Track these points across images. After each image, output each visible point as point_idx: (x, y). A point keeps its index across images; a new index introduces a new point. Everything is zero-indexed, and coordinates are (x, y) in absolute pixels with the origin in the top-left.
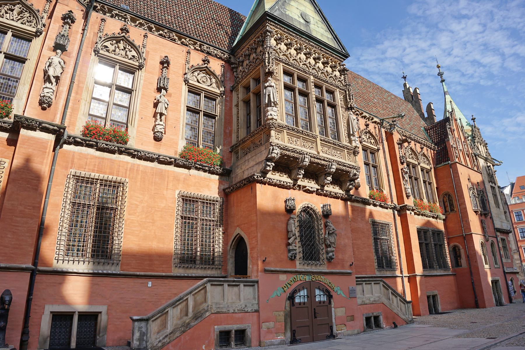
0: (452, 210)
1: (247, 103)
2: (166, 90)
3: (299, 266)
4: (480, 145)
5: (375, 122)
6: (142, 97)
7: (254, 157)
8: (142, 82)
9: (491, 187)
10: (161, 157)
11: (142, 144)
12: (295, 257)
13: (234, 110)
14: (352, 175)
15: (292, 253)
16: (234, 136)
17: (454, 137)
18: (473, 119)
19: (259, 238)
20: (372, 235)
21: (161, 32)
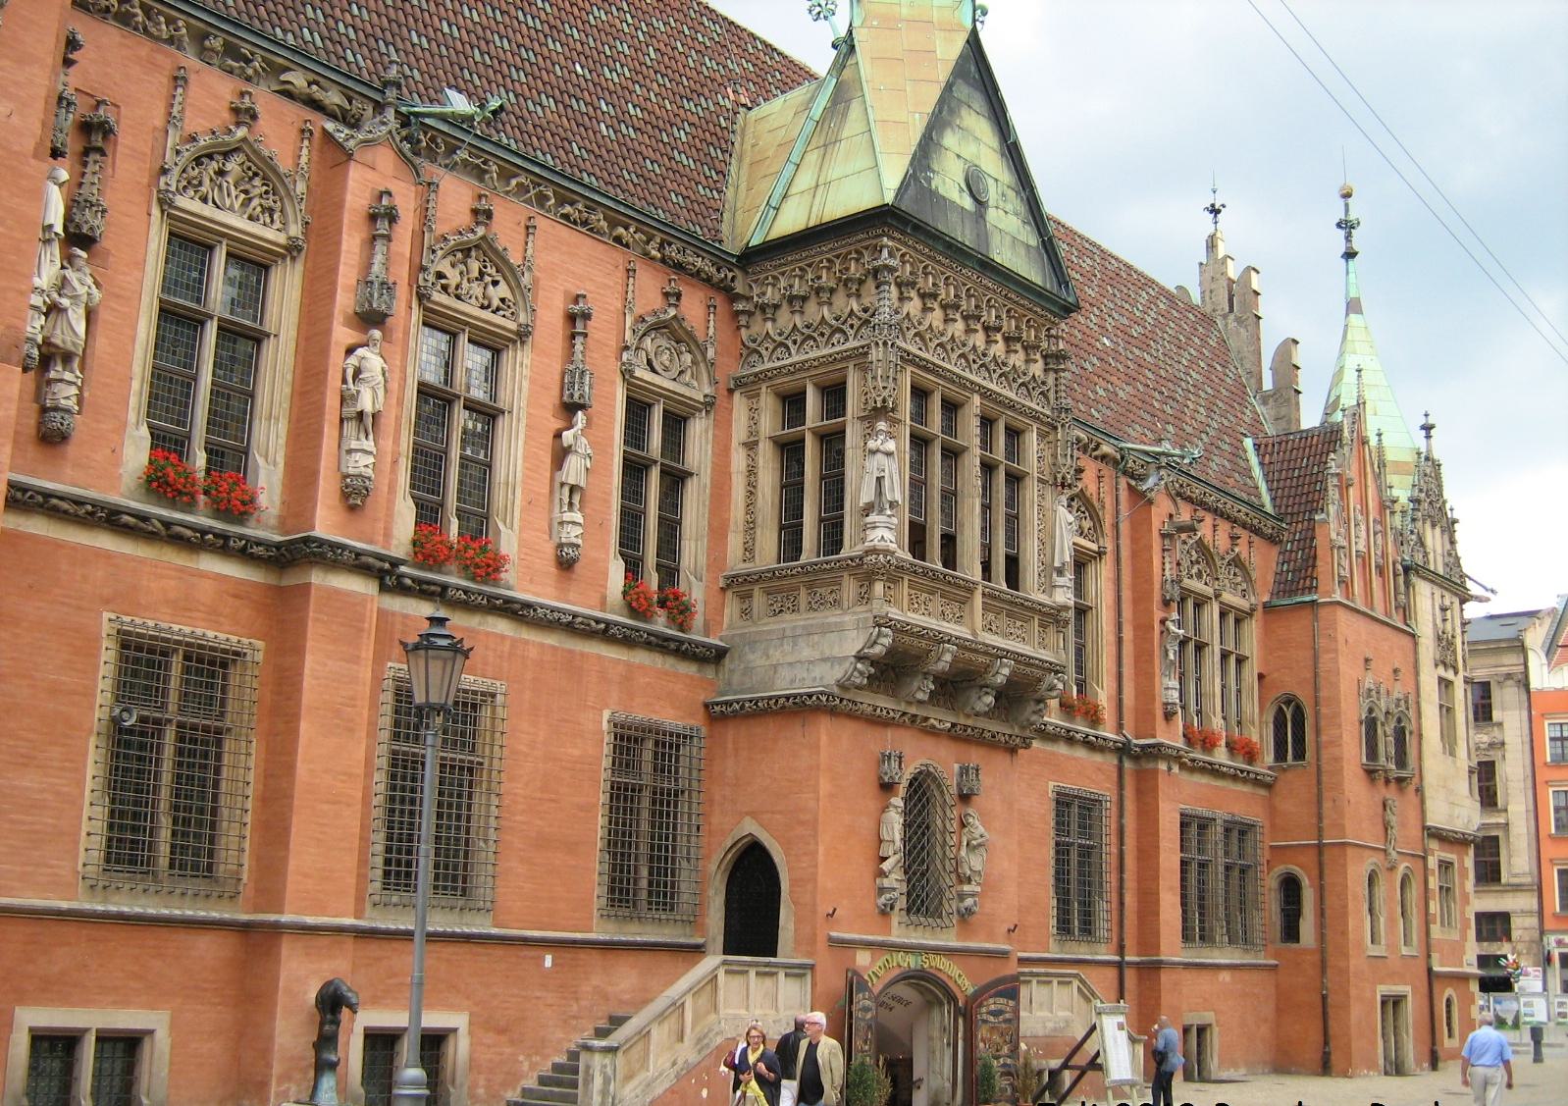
0: (1300, 754)
1: (790, 451)
3: (898, 934)
4: (1433, 526)
5: (1104, 457)
6: (527, 436)
7: (816, 637)
8: (525, 384)
9: (1441, 680)
10: (580, 619)
12: (892, 908)
13: (739, 460)
14: (1044, 686)
16: (735, 542)
17: (1344, 508)
18: (1428, 428)
19: (821, 858)
20: (1052, 833)
21: (568, 209)
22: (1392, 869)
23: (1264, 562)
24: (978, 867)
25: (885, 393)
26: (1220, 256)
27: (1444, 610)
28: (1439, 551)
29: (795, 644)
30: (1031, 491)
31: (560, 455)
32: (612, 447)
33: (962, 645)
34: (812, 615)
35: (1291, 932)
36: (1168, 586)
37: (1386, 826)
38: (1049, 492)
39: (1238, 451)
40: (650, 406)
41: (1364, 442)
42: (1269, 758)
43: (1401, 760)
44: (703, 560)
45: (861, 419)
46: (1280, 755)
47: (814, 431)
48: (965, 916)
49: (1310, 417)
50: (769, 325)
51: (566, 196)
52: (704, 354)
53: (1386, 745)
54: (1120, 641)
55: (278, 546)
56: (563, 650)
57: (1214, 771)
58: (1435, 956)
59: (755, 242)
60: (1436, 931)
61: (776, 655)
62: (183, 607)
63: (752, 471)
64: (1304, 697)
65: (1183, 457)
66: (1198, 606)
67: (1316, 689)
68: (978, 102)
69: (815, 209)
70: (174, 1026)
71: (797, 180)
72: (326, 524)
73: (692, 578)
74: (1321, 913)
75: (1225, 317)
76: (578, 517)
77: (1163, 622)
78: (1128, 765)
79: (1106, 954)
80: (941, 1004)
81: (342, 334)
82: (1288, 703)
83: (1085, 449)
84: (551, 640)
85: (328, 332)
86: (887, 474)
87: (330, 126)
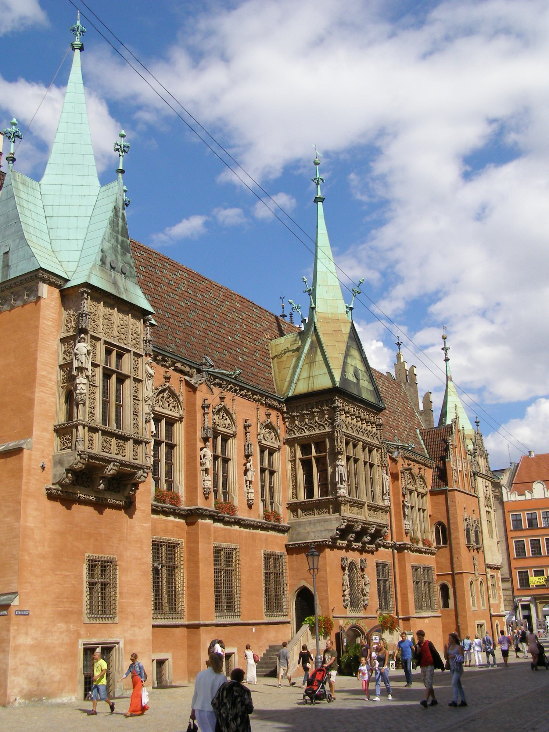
3: (349, 614)
4: (481, 457)
9: (487, 511)
14: (383, 532)
22: (477, 580)
23: (429, 474)
26: (402, 361)
28: (483, 466)
29: (315, 525)
30: (376, 469)
31: (246, 472)
35: (446, 604)
42: (435, 544)
43: (477, 542)
46: (438, 542)
48: (365, 607)
51: (239, 387)
53: (473, 538)
55: (188, 510)
57: (419, 551)
59: (290, 395)
60: (491, 599)
62: (165, 531)
64: (445, 521)
68: (355, 346)
69: (310, 385)
70: (173, 657)
71: (302, 374)
72: (201, 503)
75: (405, 384)
76: (252, 491)
77: (403, 502)
80: (360, 635)
81: (200, 444)
85: (195, 444)
87: (187, 378)
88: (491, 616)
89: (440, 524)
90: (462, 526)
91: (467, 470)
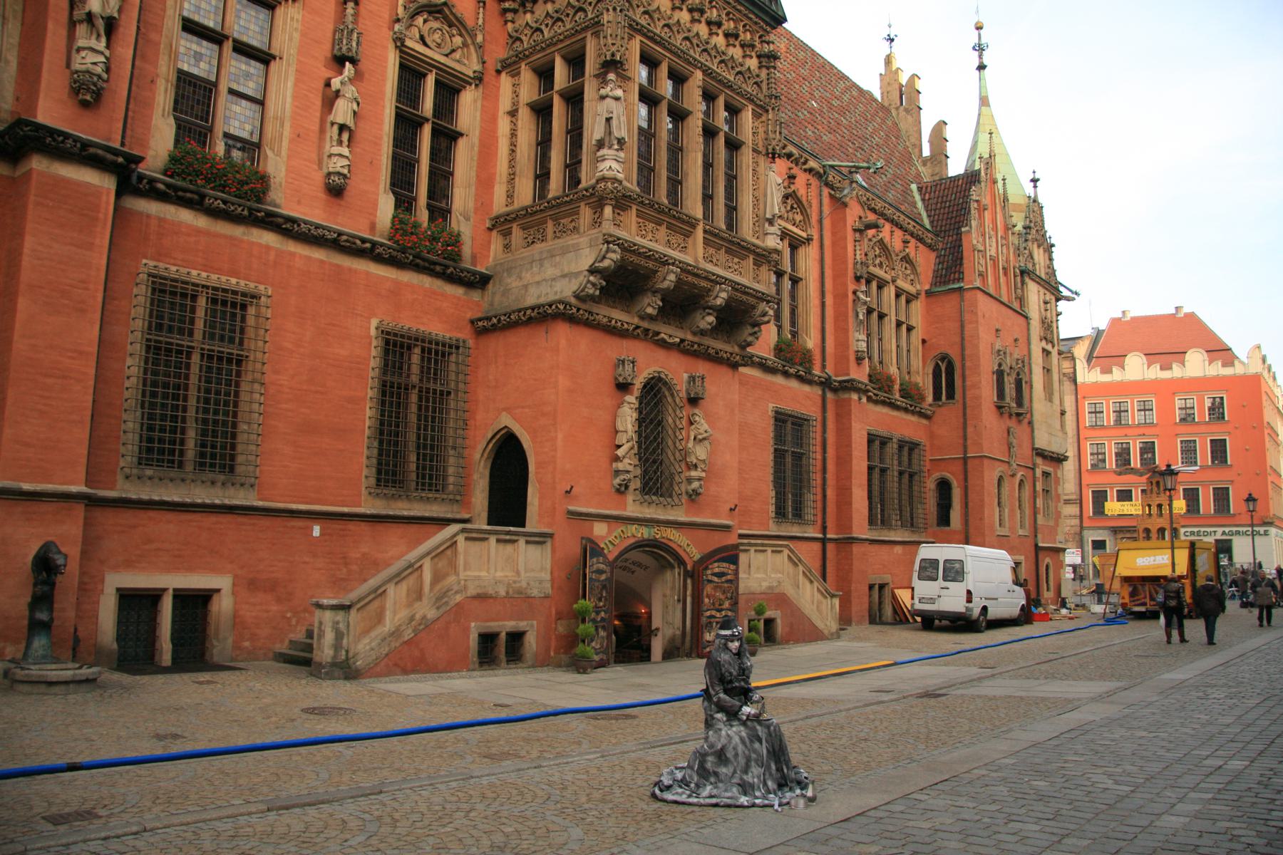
0: (951, 396)
1: (542, 111)
2: (354, 61)
3: (632, 507)
4: (1039, 246)
5: (810, 170)
7: (558, 258)
8: (296, 36)
9: (1044, 350)
10: (344, 238)
11: (299, 202)
12: (627, 487)
13: (504, 125)
14: (758, 313)
15: (622, 477)
16: (499, 192)
17: (982, 225)
19: (560, 443)
20: (772, 442)
22: (1013, 476)
23: (926, 261)
24: (703, 457)
25: (614, 49)
27: (1046, 303)
29: (542, 266)
30: (746, 157)
31: (330, 99)
32: (383, 99)
33: (685, 269)
34: (557, 241)
36: (859, 266)
37: (1010, 446)
38: (762, 160)
39: (907, 191)
40: (425, 75)
41: (995, 182)
42: (930, 399)
43: (1020, 403)
44: (471, 205)
45: (596, 76)
46: (937, 396)
47: (562, 94)
48: (694, 496)
49: (956, 167)
50: (528, 16)
52: (473, 37)
54: (823, 305)
56: (331, 264)
57: (892, 405)
58: (1039, 536)
60: (1040, 518)
61: (527, 277)
63: (513, 134)
64: (954, 355)
65: (869, 168)
66: (880, 287)
67: (963, 349)
73: (461, 218)
74: (966, 505)
75: (897, 109)
76: (345, 151)
77: (854, 293)
78: (829, 395)
79: (813, 532)
82: (943, 359)
83: (797, 162)
84: (318, 254)
86: (614, 116)
88: (1037, 548)
89: (944, 357)
90: (987, 366)
91: (1008, 261)
